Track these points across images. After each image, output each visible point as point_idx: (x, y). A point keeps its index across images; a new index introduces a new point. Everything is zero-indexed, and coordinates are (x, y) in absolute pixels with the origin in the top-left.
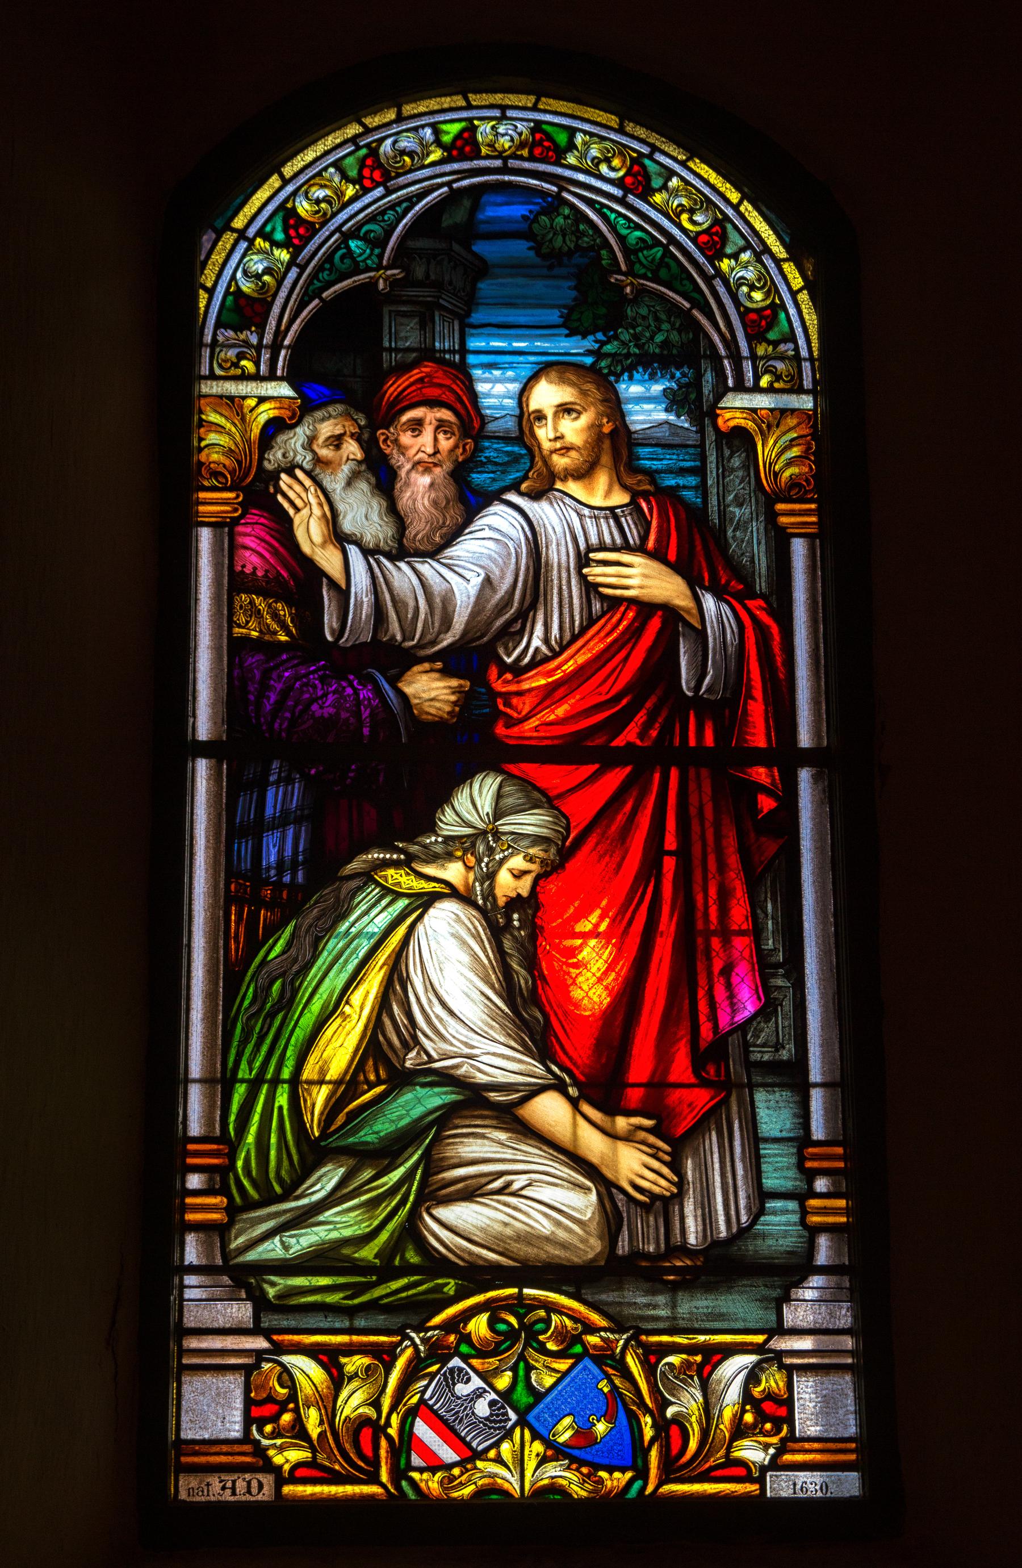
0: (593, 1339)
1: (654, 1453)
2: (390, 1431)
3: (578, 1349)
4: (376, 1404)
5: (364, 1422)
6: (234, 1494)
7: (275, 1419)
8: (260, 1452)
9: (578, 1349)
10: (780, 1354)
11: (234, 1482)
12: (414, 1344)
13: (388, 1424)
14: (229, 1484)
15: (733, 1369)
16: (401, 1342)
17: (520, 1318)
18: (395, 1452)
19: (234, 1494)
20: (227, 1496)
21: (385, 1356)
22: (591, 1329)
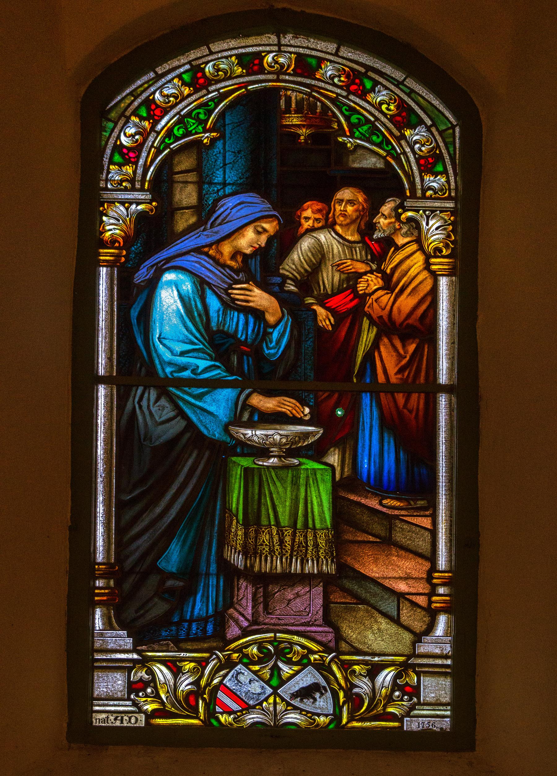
1: (345, 708)
2: (205, 696)
3: (305, 661)
5: (190, 693)
6: (122, 722)
7: (144, 690)
9: (305, 661)
10: (413, 666)
11: (122, 718)
12: (218, 657)
14: (119, 718)
16: (211, 656)
17: (275, 647)
18: (207, 705)
19: (122, 722)
20: (118, 723)
21: (202, 663)
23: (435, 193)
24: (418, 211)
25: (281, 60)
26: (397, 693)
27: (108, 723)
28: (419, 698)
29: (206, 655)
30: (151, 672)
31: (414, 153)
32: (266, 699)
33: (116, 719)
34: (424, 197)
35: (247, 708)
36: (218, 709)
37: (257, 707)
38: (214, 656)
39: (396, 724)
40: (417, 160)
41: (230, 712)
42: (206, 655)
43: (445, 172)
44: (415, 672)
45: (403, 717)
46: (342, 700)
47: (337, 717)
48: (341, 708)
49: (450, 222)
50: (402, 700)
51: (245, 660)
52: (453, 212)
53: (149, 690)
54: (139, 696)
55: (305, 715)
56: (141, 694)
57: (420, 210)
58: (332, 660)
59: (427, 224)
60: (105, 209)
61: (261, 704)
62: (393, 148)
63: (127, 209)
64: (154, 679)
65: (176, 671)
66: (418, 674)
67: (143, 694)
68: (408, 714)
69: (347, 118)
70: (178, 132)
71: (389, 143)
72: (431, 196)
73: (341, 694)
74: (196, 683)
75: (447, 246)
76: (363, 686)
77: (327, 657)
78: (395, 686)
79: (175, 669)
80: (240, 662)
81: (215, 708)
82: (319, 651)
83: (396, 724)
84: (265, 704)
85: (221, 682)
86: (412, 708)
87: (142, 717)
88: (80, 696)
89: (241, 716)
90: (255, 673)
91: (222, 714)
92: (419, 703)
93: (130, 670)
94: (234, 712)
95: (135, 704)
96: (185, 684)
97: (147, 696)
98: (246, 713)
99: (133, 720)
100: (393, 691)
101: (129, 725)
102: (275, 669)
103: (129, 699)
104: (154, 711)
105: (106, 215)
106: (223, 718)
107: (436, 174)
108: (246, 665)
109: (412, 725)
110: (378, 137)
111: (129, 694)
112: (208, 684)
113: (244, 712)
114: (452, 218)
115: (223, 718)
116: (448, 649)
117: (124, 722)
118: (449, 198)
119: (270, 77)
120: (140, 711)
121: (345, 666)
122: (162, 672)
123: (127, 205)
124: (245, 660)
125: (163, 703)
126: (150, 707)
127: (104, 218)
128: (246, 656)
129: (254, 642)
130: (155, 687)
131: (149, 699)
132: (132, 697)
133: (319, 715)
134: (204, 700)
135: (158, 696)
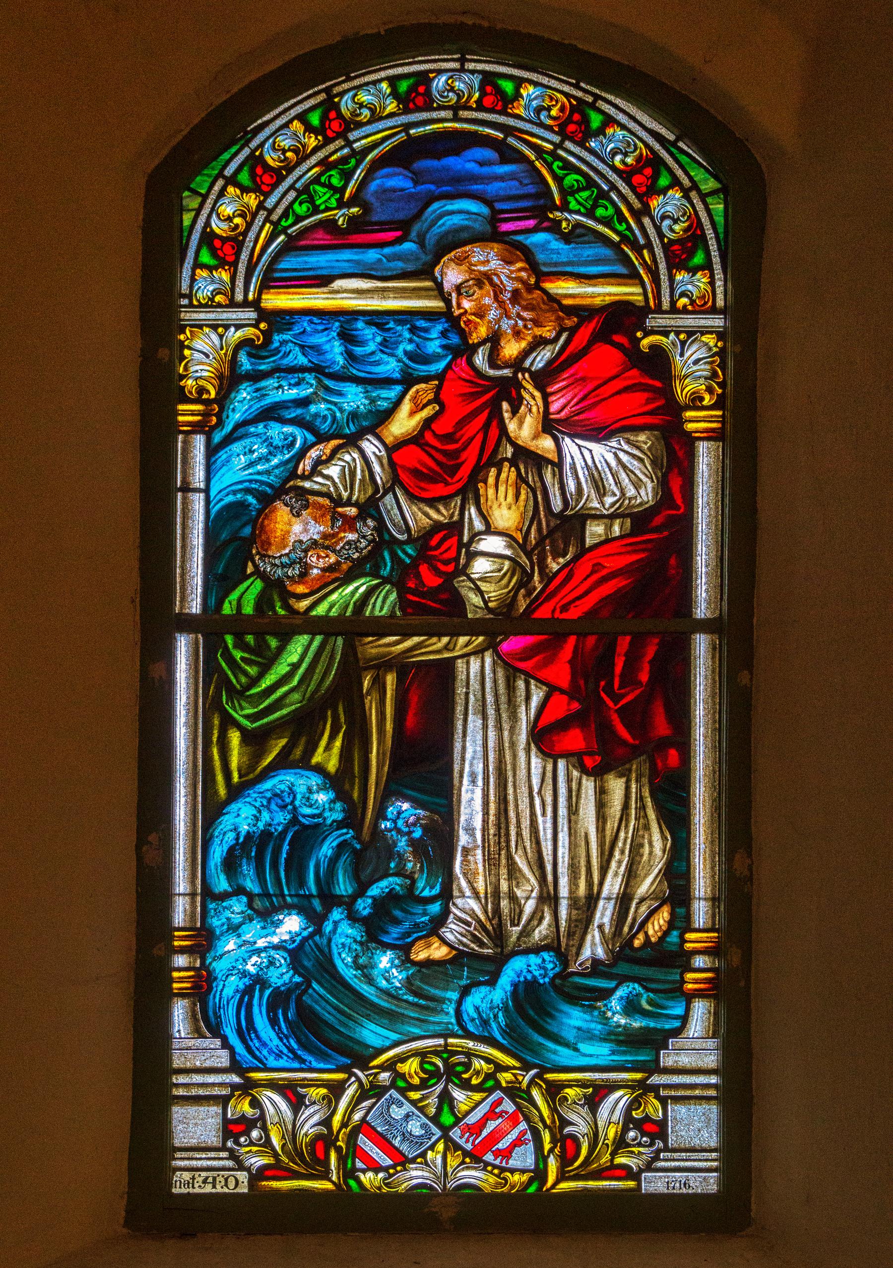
0: (505, 1077)
2: (338, 1143)
3: (490, 1083)
4: (326, 1122)
5: (318, 1137)
6: (214, 1187)
7: (247, 1133)
8: (233, 1156)
10: (655, 1089)
11: (214, 1179)
12: (358, 1079)
13: (337, 1139)
14: (210, 1180)
15: (619, 1099)
16: (349, 1078)
17: (445, 1061)
18: (342, 1159)
19: (214, 1187)
20: (208, 1189)
21: (336, 1090)
22: (501, 1068)
23: (693, 302)
24: (666, 334)
25: (459, 85)
26: (632, 1134)
27: (193, 1187)
28: (665, 1142)
29: (340, 1076)
30: (255, 1103)
31: (661, 235)
32: (432, 1148)
33: (205, 1181)
34: (674, 309)
35: (402, 1161)
36: (359, 1164)
37: (419, 1160)
38: (353, 1079)
39: (631, 1184)
40: (666, 248)
41: (376, 1168)
42: (340, 1076)
43: (708, 266)
44: (658, 1097)
45: (641, 1171)
46: (547, 1146)
47: (540, 1174)
48: (545, 1159)
49: (715, 350)
50: (640, 1145)
51: (401, 1084)
52: (721, 336)
53: (255, 1134)
54: (239, 1145)
55: (491, 1172)
56: (242, 1139)
57: (670, 332)
58: (532, 1082)
59: (682, 355)
60: (188, 339)
61: (423, 1155)
62: (629, 228)
63: (221, 337)
64: (262, 1117)
65: (297, 1103)
66: (663, 1101)
67: (246, 1141)
68: (649, 1167)
69: (559, 180)
70: (301, 209)
71: (622, 219)
72: (685, 306)
73: (547, 1137)
74: (326, 1122)
75: (710, 390)
76: (579, 1125)
77: (524, 1076)
78: (628, 1121)
79: (293, 1098)
80: (393, 1085)
81: (354, 1163)
82: (514, 1068)
83: (631, 1184)
84: (430, 1154)
85: (363, 1120)
86: (656, 1158)
87: (243, 1176)
88: (150, 1144)
89: (394, 1174)
90: (414, 1103)
91: (364, 1171)
92: (666, 1149)
93: (224, 1101)
94: (386, 1169)
95: (233, 1156)
96: (309, 1123)
97: (251, 1144)
98: (401, 1171)
99: (232, 1185)
100: (625, 1130)
101: (226, 1190)
102: (446, 1098)
103: (224, 1148)
104: (263, 1168)
105: (189, 348)
106: (367, 1178)
107: (694, 271)
108: (403, 1091)
109: (655, 1184)
110: (606, 208)
111: (224, 1141)
112: (344, 1125)
113: (399, 1168)
114: (719, 344)
115: (367, 1178)
116: (711, 1060)
117: (218, 1187)
118: (714, 310)
119: (443, 114)
120: (241, 1167)
121: (554, 1091)
122: (275, 1104)
123: (220, 330)
124: (401, 1084)
125: (275, 1155)
126: (257, 1161)
127: (187, 352)
128: (403, 1076)
129: (416, 1053)
130: (264, 1128)
131: (255, 1149)
132: (229, 1144)
133: (512, 1171)
134: (339, 1150)
135: (268, 1143)
